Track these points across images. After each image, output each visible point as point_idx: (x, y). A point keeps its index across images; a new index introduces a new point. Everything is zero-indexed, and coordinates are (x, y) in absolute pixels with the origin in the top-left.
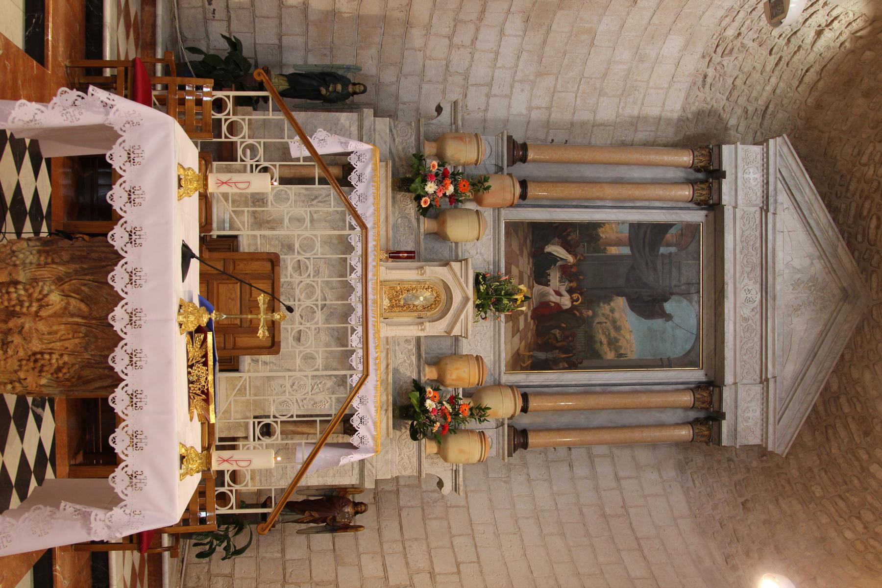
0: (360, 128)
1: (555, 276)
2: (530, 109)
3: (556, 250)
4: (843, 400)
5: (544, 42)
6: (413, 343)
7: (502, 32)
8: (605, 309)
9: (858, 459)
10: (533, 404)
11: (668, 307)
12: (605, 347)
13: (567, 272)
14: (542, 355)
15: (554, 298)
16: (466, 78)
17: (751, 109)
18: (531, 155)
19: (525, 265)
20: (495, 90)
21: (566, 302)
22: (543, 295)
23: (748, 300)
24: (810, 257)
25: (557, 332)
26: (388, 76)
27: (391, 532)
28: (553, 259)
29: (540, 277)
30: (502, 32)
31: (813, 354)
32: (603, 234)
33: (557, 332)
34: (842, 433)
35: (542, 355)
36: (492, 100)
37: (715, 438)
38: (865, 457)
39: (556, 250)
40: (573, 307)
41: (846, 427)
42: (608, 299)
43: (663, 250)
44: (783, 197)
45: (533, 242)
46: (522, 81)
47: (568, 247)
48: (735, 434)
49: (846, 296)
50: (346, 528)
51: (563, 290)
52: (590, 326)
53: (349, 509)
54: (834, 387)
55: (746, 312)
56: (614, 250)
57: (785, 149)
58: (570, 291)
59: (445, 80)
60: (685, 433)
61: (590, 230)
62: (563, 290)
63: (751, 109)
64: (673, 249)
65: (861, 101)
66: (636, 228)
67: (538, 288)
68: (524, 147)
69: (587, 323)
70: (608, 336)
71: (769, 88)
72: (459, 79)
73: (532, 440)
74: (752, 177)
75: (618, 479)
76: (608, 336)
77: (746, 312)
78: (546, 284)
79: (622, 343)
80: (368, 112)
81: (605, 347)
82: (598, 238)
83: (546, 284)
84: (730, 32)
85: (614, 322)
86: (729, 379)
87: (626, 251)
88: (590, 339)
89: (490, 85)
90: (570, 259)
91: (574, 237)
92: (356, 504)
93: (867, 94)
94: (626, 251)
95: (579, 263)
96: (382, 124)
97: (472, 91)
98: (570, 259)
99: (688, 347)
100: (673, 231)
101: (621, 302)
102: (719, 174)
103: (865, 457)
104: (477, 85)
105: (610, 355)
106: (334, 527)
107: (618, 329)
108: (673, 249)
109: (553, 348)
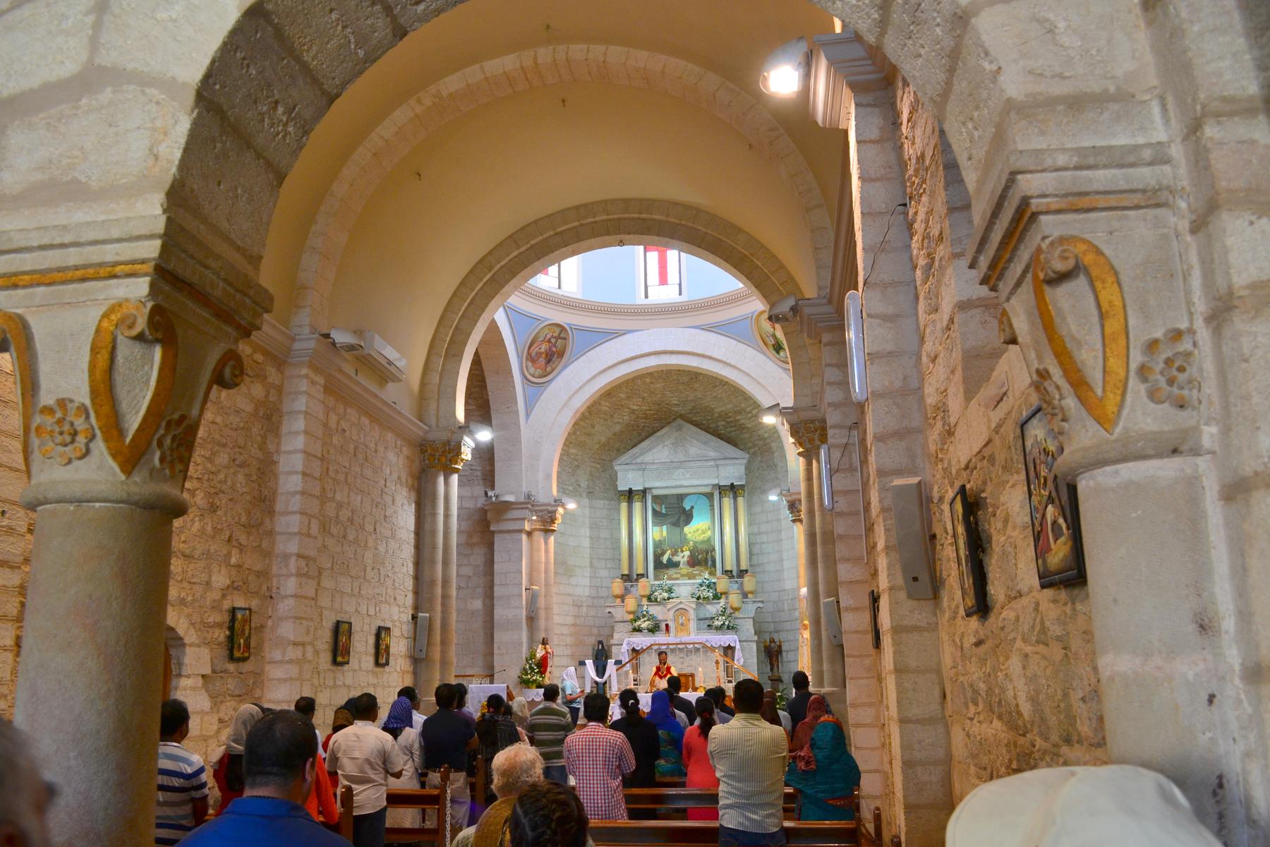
0: (618, 645)
1: (676, 559)
2: (606, 568)
3: (665, 559)
4: (729, 420)
5: (579, 567)
6: (702, 622)
7: (577, 585)
8: (689, 536)
9: (751, 417)
10: (728, 568)
11: (688, 508)
12: (706, 535)
13: (675, 553)
14: (710, 563)
15: (686, 559)
16: (595, 598)
17: (601, 470)
18: (626, 572)
19: (672, 571)
20: (599, 584)
21: (687, 553)
22: (684, 563)
23: (683, 474)
24: (664, 446)
25: (700, 557)
26: (595, 631)
27: (788, 626)
28: (669, 560)
29: (676, 565)
30: (577, 585)
31: (705, 443)
32: (657, 538)
33: (700, 557)
34: (742, 422)
35: (710, 563)
36: (604, 585)
37: (742, 486)
38: (750, 415)
39: (665, 559)
40: (689, 550)
41: (738, 420)
42: (685, 535)
43: (664, 511)
44: (639, 460)
45: (662, 568)
46: (595, 573)
47: (663, 553)
48: (740, 478)
49: (680, 428)
50: (780, 646)
51: (682, 555)
52: (697, 542)
53: (773, 645)
54: (723, 423)
55: (688, 476)
56: (665, 534)
57: (619, 462)
58: (682, 551)
59: (597, 607)
60: (740, 500)
61: (657, 545)
62: (682, 555)
63: (601, 470)
64: (663, 506)
65: (596, 428)
66: (655, 524)
67: (681, 566)
68: (622, 575)
69: (695, 543)
70: (701, 534)
71: (593, 464)
72: (595, 601)
73: (743, 567)
74: (630, 475)
75: (767, 522)
76: (701, 534)
77: (688, 476)
78: (679, 562)
79: (703, 528)
80: (612, 642)
81: (706, 535)
82: (660, 541)
83: (679, 562)
84: (571, 488)
85: (694, 532)
86: (716, 482)
87: (665, 527)
88: (703, 542)
89: (597, 587)
90: (669, 552)
91: (659, 551)
92: (770, 642)
93: (593, 426)
94: (665, 527)
95: (670, 548)
96: (616, 636)
97: (600, 595)
98: (669, 552)
99: (705, 498)
100: (655, 507)
101: (686, 529)
102: (630, 491)
103: (750, 415)
104: (598, 593)
105: (709, 533)
106: (779, 651)
107: (698, 530)
108: (663, 506)
109: (706, 559)
